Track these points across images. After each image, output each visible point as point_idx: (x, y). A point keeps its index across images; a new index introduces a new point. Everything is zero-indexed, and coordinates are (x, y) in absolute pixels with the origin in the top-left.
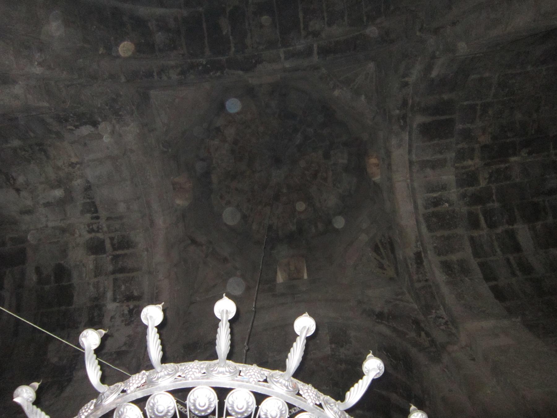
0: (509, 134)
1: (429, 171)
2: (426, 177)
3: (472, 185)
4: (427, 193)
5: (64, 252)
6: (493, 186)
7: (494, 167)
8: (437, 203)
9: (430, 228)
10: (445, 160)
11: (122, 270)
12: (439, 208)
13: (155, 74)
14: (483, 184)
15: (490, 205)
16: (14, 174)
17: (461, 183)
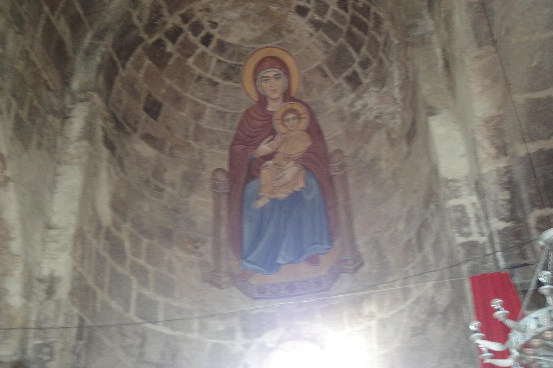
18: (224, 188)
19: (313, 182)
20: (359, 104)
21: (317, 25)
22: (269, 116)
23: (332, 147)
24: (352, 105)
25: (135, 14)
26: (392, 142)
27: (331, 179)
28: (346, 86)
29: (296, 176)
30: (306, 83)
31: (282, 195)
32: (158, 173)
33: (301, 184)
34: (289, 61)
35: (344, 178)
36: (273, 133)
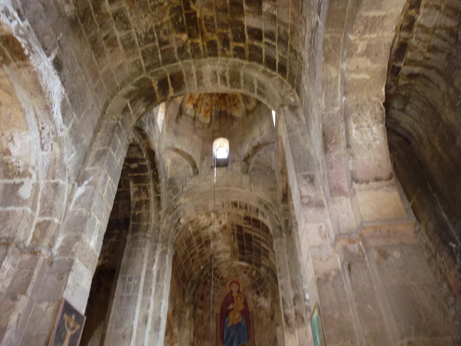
0: (180, 20)
1: (204, 81)
2: (208, 82)
3: (216, 44)
4: (218, 83)
5: (239, 215)
6: (219, 30)
7: (205, 28)
8: (224, 79)
9: (239, 87)
10: (197, 73)
11: (246, 208)
12: (228, 78)
13: (158, 196)
14: (215, 38)
15: (230, 36)
16: (204, 227)
17: (214, 54)
18: (219, 320)
19: (244, 320)
20: (258, 300)
21: (249, 276)
22: (233, 297)
23: (250, 310)
24: (257, 299)
25: (201, 278)
26: (267, 316)
27: (249, 320)
28: (255, 294)
29: (239, 318)
30: (244, 290)
31: (235, 323)
32: (202, 317)
33: (240, 320)
34: (240, 283)
35: (253, 320)
36: (233, 302)
